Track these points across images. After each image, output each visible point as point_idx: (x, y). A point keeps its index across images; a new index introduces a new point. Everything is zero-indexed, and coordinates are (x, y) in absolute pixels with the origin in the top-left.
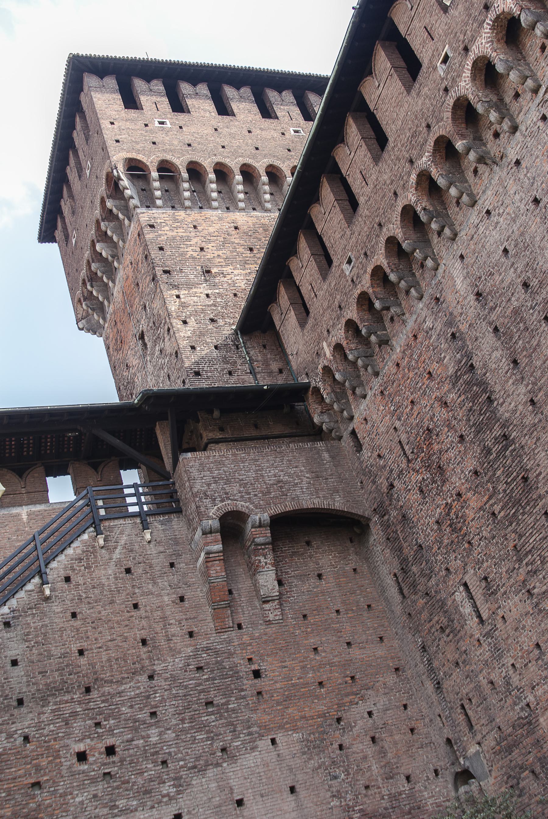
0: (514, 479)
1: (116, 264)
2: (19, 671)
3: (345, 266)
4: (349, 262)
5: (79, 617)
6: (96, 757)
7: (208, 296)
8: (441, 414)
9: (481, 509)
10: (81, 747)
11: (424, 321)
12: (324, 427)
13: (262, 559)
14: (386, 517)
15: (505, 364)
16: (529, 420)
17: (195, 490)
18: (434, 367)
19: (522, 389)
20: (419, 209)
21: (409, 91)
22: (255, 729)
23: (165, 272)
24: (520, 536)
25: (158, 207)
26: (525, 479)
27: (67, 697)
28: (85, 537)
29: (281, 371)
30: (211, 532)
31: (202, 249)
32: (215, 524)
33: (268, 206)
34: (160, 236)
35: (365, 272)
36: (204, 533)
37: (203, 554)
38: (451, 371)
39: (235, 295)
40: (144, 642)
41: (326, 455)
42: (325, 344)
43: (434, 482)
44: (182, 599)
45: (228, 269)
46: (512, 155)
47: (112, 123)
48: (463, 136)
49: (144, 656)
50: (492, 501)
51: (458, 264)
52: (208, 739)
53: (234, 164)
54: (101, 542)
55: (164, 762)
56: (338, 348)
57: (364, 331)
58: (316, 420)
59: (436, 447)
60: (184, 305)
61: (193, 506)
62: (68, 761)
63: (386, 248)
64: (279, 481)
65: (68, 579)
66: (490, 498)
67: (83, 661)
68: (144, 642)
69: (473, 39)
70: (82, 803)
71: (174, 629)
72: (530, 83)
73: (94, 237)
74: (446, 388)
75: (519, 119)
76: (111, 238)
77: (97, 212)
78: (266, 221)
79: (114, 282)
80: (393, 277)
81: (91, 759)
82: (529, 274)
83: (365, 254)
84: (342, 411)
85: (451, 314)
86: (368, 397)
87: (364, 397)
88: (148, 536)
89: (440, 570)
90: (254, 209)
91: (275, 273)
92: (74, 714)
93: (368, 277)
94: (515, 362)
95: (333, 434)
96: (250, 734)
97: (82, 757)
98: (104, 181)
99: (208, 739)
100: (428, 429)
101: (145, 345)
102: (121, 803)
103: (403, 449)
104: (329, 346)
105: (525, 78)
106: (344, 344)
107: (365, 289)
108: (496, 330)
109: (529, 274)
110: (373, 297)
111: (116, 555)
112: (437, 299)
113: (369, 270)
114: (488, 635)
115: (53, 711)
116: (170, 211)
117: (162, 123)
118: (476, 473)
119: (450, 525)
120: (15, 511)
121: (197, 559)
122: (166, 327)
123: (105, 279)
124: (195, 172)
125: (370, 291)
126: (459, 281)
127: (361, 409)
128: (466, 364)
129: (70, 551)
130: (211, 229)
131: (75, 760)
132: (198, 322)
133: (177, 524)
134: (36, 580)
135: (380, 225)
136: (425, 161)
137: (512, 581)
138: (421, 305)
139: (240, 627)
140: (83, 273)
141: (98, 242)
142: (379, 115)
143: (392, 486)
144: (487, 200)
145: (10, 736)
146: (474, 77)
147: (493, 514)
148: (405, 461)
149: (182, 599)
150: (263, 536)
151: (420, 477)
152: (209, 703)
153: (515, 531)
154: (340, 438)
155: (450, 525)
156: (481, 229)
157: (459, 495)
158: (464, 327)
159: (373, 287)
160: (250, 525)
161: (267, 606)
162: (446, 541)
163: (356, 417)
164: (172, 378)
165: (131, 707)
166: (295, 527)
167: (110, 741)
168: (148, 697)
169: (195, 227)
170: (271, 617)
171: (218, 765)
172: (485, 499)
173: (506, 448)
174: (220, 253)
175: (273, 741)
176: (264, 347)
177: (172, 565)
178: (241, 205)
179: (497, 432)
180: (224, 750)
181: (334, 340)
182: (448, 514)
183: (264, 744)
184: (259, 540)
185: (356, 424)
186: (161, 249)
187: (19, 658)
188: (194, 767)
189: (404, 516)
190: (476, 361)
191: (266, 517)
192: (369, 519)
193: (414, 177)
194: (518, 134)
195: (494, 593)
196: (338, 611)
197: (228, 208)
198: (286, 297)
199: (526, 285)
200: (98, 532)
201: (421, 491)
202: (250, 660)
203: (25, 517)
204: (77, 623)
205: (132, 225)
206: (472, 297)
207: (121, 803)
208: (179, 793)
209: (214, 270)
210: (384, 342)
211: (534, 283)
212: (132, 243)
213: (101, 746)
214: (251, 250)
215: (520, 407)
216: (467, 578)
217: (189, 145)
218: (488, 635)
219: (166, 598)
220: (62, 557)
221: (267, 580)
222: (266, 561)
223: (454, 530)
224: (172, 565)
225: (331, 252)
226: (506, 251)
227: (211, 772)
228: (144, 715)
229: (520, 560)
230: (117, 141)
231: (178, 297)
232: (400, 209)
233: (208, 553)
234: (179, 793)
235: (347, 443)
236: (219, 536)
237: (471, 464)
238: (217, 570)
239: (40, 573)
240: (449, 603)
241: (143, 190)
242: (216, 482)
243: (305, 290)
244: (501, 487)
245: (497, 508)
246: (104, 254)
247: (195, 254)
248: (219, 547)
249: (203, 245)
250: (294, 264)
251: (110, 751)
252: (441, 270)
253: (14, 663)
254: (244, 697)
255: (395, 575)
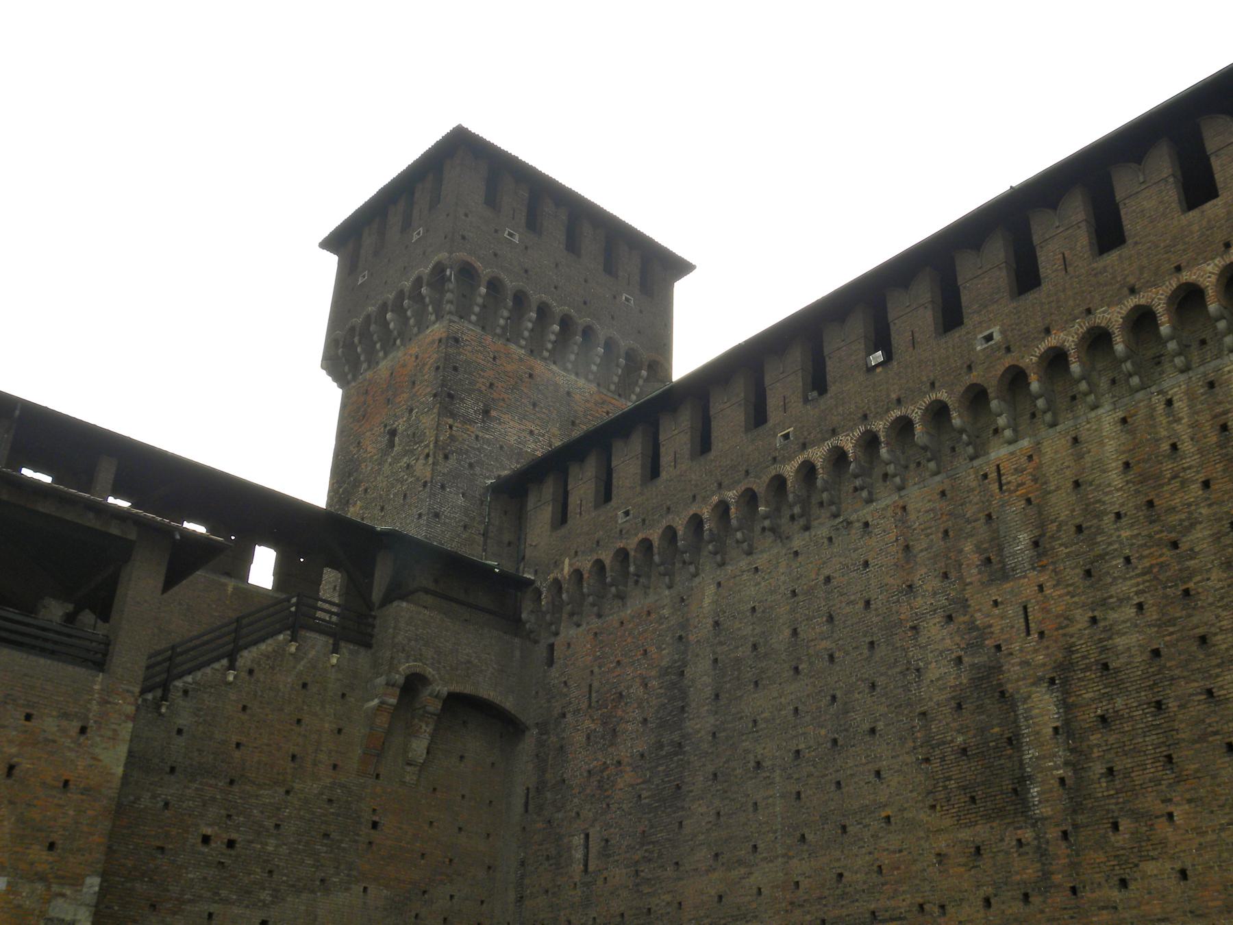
0: (669, 782)
1: (398, 342)
2: (181, 741)
3: (620, 513)
4: (627, 513)
5: (248, 711)
6: (218, 845)
7: (477, 437)
8: (637, 690)
9: (631, 785)
10: (209, 831)
11: (663, 607)
12: (527, 626)
13: (424, 727)
14: (545, 737)
15: (709, 692)
16: (705, 746)
17: (396, 640)
18: (653, 650)
19: (712, 720)
20: (706, 527)
21: (747, 430)
22: (354, 873)
23: (451, 396)
24: (652, 827)
25: (470, 322)
26: (678, 787)
27: (212, 782)
28: (281, 637)
29: (509, 544)
30: (393, 685)
31: (491, 385)
32: (399, 678)
33: (569, 366)
34: (460, 354)
35: (636, 535)
36: (387, 684)
37: (376, 701)
38: (664, 663)
39: (501, 447)
40: (294, 757)
41: (517, 653)
42: (567, 561)
43: (603, 737)
44: (340, 731)
45: (506, 418)
46: (797, 543)
47: (466, 215)
48: (767, 504)
49: (289, 771)
50: (643, 786)
51: (713, 588)
52: (313, 866)
53: (558, 309)
54: (293, 649)
55: (270, 872)
56: (578, 574)
57: (609, 580)
58: (524, 616)
59: (620, 713)
60: (452, 438)
61: (388, 654)
62: (194, 840)
63: (664, 532)
64: (469, 662)
65: (251, 672)
66: (643, 783)
67: (237, 754)
68: (294, 757)
69: (813, 444)
70: (192, 880)
71: (322, 757)
72: (834, 508)
73: (390, 303)
74: (653, 673)
75: (815, 523)
76: (408, 319)
77: (407, 284)
78: (559, 380)
79: (386, 355)
80: (656, 558)
81: (213, 845)
82: (762, 641)
83: (644, 520)
84: (551, 624)
85: (688, 620)
86: (581, 629)
87: (578, 625)
88: (334, 661)
89: (571, 810)
90: (555, 363)
91: (553, 467)
92: (213, 799)
93: (636, 540)
94: (717, 696)
95: (532, 636)
96: (348, 875)
97: (206, 840)
98: (431, 266)
99: (313, 866)
100: (621, 694)
101: (391, 444)
102: (224, 893)
103: (590, 697)
104: (570, 565)
105: (832, 503)
106: (586, 576)
107: (628, 548)
108: (716, 661)
109: (762, 641)
110: (631, 560)
111: (300, 667)
112: (683, 600)
113: (641, 536)
114: (585, 884)
115: (197, 789)
116: (479, 330)
117: (510, 234)
118: (642, 755)
119: (599, 781)
120: (224, 580)
121: (368, 701)
122: (427, 451)
123: (378, 346)
124: (520, 299)
125: (632, 553)
126: (707, 601)
127: (569, 632)
128: (679, 667)
129: (263, 646)
130: (509, 368)
131: (199, 840)
132: (459, 461)
133: (364, 659)
134: (225, 662)
135: (669, 509)
136: (731, 495)
137: (628, 855)
138: (667, 592)
139: (378, 776)
140: (358, 321)
141: (392, 311)
142: (714, 424)
143: (564, 715)
144: (761, 560)
145: (154, 797)
146: (798, 471)
147: (640, 796)
148: (586, 704)
149: (340, 731)
150: (435, 706)
151: (593, 726)
152: (326, 835)
153: (650, 821)
154: (536, 642)
155: (599, 781)
156: (745, 577)
157: (619, 763)
158: (692, 638)
159: (635, 551)
160: (428, 692)
161: (409, 769)
162: (588, 791)
163: (562, 635)
164: (408, 501)
165: (262, 812)
166: (464, 707)
167: (234, 836)
168: (279, 809)
169: (494, 358)
170: (407, 778)
171: (313, 892)
172: (640, 781)
173: (676, 754)
174: (506, 396)
175: (365, 889)
176: (506, 513)
177: (343, 695)
178: (546, 354)
179: (676, 737)
180: (322, 881)
181: (578, 565)
182: (602, 772)
183: (357, 889)
184: (431, 709)
185: (559, 642)
186: (455, 369)
187: (185, 729)
188: (293, 886)
189: (562, 747)
190: (688, 672)
191: (445, 691)
192: (528, 728)
193: (715, 499)
194: (807, 533)
195: (609, 856)
196: (463, 796)
197: (532, 351)
198: (551, 490)
199: (755, 647)
200: (294, 639)
201: (588, 738)
202: (374, 810)
203: (230, 589)
204: (245, 717)
205: (437, 325)
206: (710, 621)
207: (224, 893)
208: (273, 902)
209: (493, 413)
210: (621, 597)
211: (762, 650)
212: (427, 341)
213: (225, 837)
214: (534, 405)
215: (703, 732)
216: (592, 831)
217: (526, 271)
218: (585, 884)
219: (327, 725)
220: (254, 649)
221: (419, 747)
222: (426, 729)
223: (600, 787)
224: (343, 695)
225: (614, 492)
226: (754, 609)
227: (304, 896)
228: (269, 824)
229: (643, 845)
230: (463, 238)
231: (451, 427)
232: (691, 513)
233: (382, 703)
234: (273, 902)
235: (541, 651)
236: (398, 691)
237: (641, 746)
238: (383, 720)
239: (232, 657)
240: (565, 841)
241: (464, 296)
242: (416, 640)
243: (573, 500)
244: (656, 781)
245: (644, 794)
246: (392, 326)
247: (483, 388)
248: (393, 701)
249: (495, 381)
250: (574, 470)
251: (231, 844)
252: (697, 580)
253: (180, 732)
254: (356, 841)
255: (528, 789)
